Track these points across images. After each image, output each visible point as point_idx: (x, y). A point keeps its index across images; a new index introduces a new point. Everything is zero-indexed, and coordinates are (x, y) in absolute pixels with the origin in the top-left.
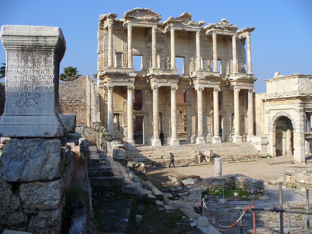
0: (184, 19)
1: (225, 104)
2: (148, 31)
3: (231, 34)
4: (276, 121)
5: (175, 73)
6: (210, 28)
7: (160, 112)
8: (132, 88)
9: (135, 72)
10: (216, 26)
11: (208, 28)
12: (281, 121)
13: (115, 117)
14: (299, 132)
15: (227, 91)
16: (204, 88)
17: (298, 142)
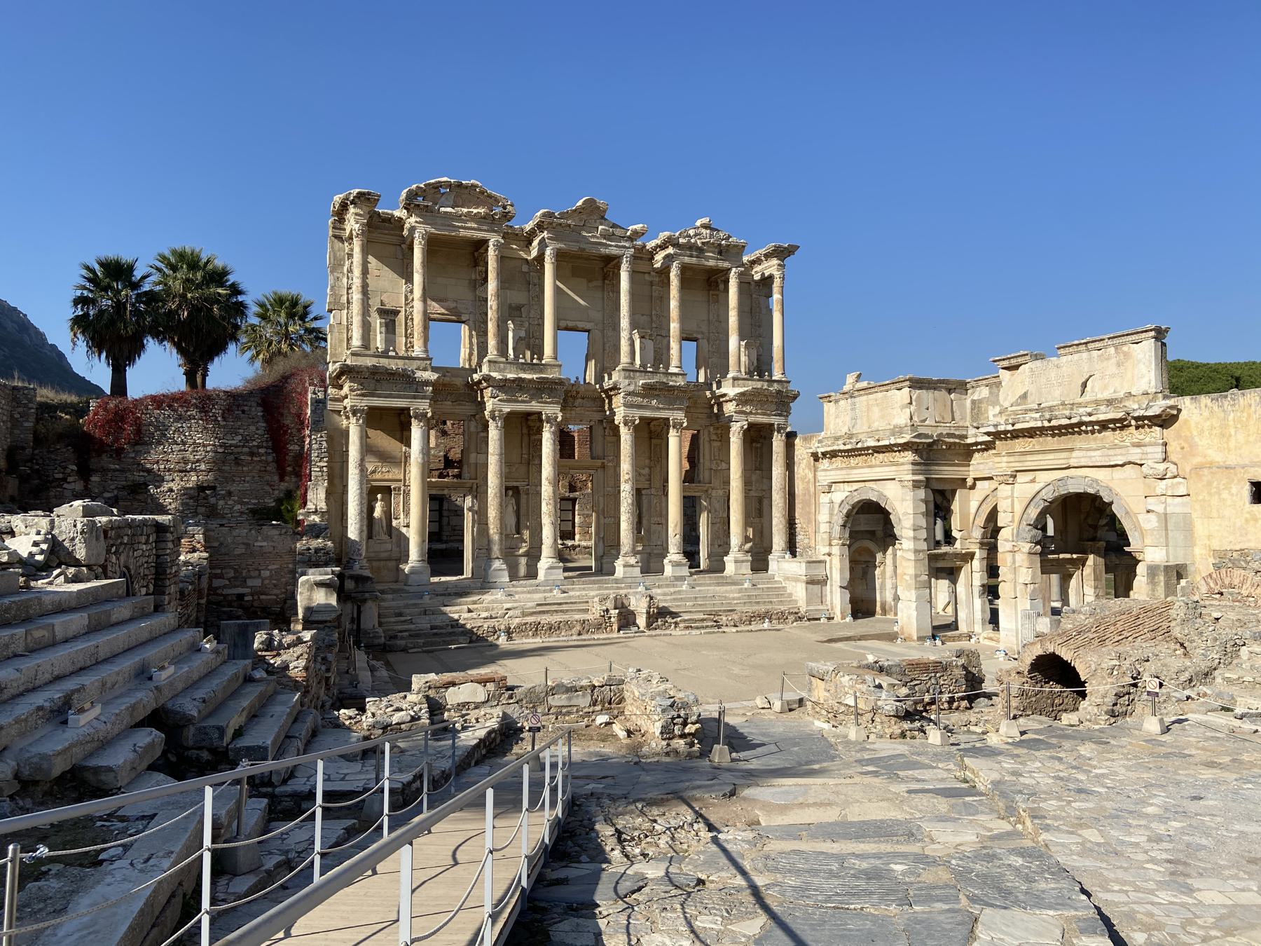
0: (584, 217)
1: (707, 464)
2: (482, 251)
3: (726, 265)
4: (848, 515)
5: (551, 375)
6: (663, 247)
7: (515, 484)
8: (421, 417)
9: (434, 369)
10: (681, 240)
11: (657, 246)
12: (867, 516)
13: (379, 496)
14: (912, 547)
15: (711, 429)
16: (641, 418)
17: (907, 578)
